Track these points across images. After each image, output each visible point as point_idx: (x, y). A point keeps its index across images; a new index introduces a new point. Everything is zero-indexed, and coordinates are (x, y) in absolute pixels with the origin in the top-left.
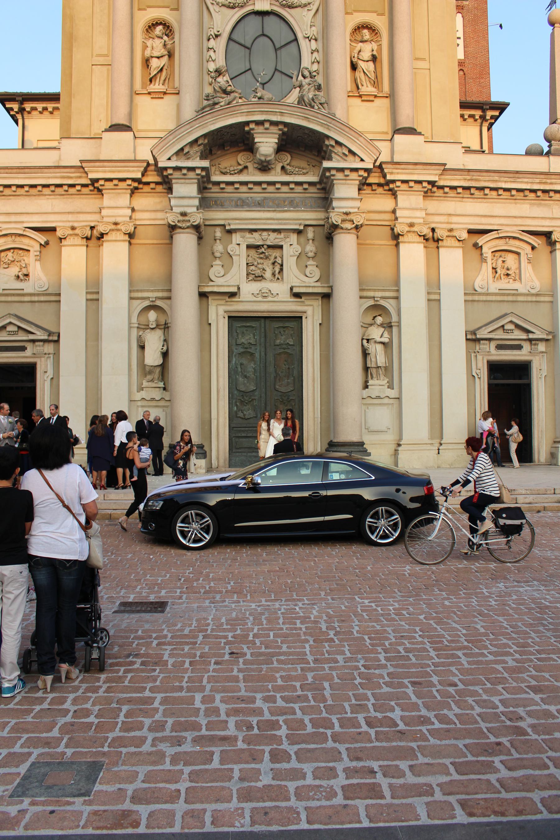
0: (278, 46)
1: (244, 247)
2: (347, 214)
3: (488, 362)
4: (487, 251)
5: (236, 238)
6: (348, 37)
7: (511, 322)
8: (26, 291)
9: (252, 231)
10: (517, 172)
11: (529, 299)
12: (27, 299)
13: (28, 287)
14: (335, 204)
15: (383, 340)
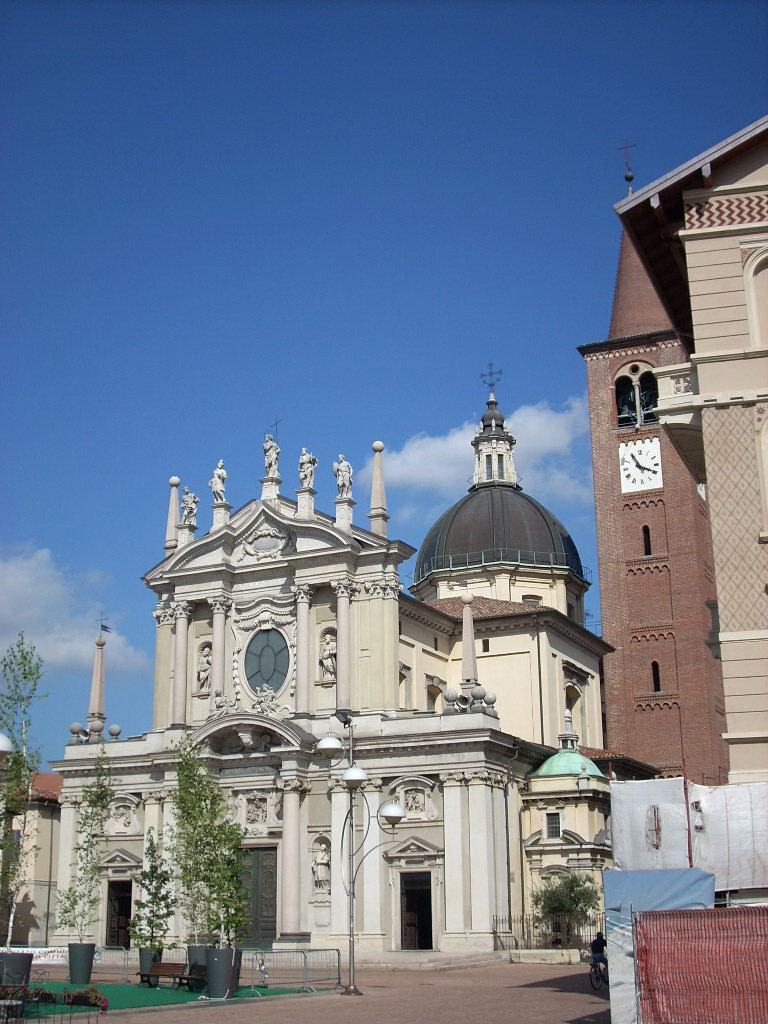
0: (276, 651)
1: (245, 800)
2: (286, 781)
3: (401, 874)
4: (400, 792)
5: (240, 796)
6: (318, 639)
7: (413, 844)
8: (129, 833)
9: (248, 791)
10: (406, 736)
11: (430, 824)
12: (128, 838)
13: (129, 831)
14: (282, 774)
15: (323, 861)
